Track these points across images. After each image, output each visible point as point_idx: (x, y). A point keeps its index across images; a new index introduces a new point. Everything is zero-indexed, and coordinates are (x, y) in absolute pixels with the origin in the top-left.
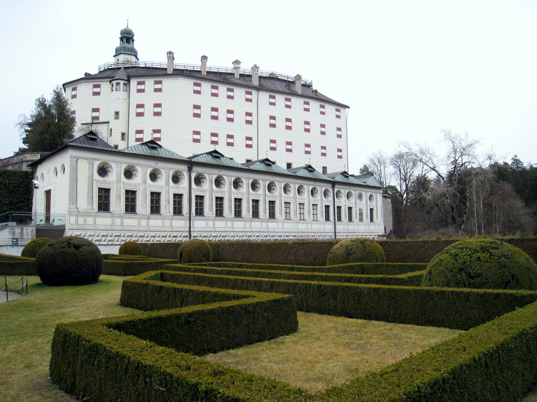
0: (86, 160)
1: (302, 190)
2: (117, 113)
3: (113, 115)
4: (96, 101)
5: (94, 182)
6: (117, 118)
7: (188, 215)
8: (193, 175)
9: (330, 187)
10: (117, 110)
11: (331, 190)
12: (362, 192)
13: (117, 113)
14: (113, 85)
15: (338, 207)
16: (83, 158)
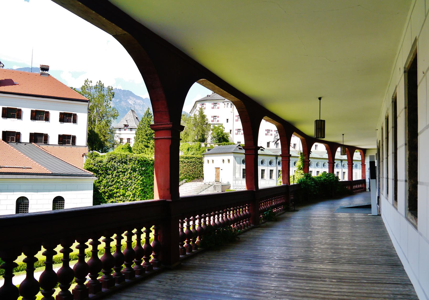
0: (239, 158)
1: (325, 164)
2: (227, 120)
3: (226, 121)
4: (215, 112)
5: (241, 167)
6: (227, 122)
7: (276, 179)
8: (278, 161)
9: (340, 162)
10: (227, 119)
11: (340, 164)
12: (357, 164)
13: (227, 120)
14: (225, 104)
15: (343, 172)
16: (237, 157)
